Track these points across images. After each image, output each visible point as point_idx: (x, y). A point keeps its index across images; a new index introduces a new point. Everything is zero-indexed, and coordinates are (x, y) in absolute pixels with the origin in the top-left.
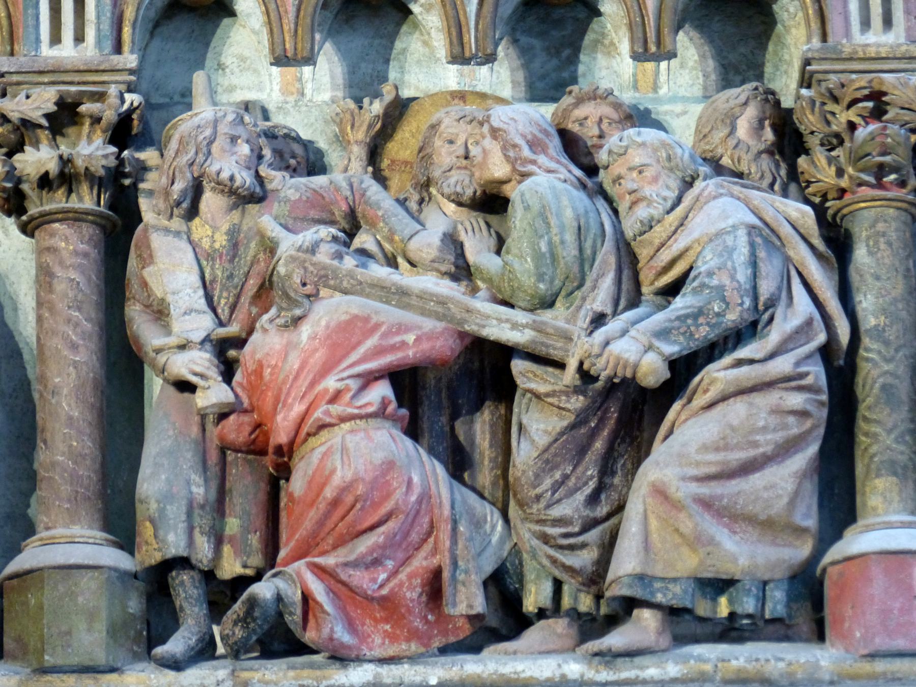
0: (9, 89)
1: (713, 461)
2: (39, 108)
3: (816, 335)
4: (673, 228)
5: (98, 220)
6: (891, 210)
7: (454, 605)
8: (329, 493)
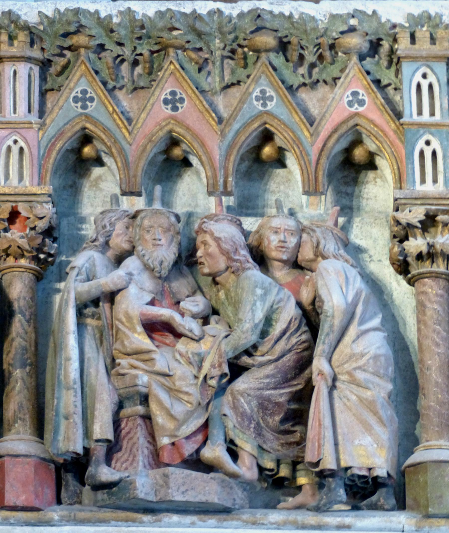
0: (400, 208)
2: (416, 217)
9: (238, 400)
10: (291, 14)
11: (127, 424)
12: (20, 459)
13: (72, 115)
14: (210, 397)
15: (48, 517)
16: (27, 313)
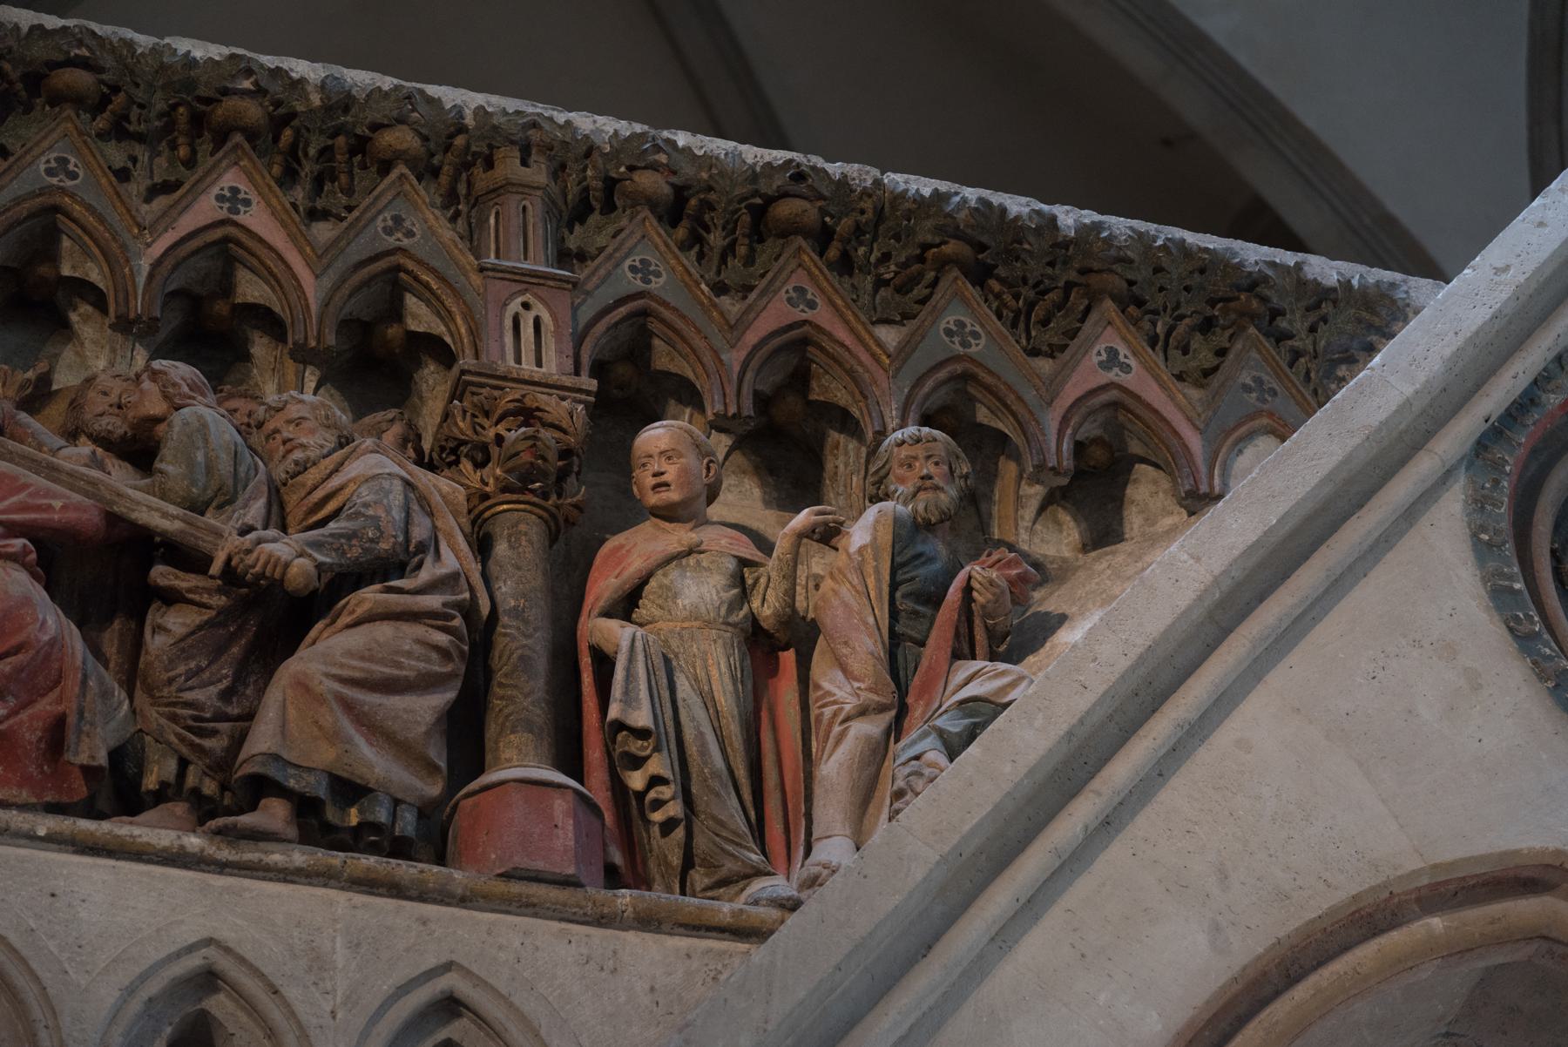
1: (357, 669)
3: (461, 593)
4: (328, 471)
6: (533, 517)
7: (77, 754)
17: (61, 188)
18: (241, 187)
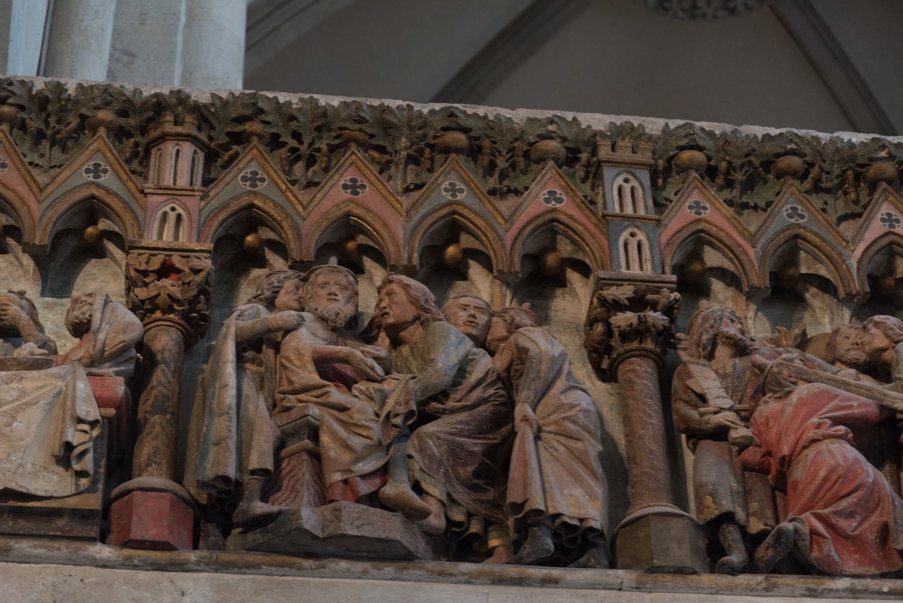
5: (657, 358)
8: (822, 474)
9: (426, 443)
10: (486, 114)
11: (289, 463)
12: (154, 494)
13: (239, 191)
14: (392, 437)
15: (183, 557)
16: (172, 365)
17: (798, 224)
18: (892, 212)
